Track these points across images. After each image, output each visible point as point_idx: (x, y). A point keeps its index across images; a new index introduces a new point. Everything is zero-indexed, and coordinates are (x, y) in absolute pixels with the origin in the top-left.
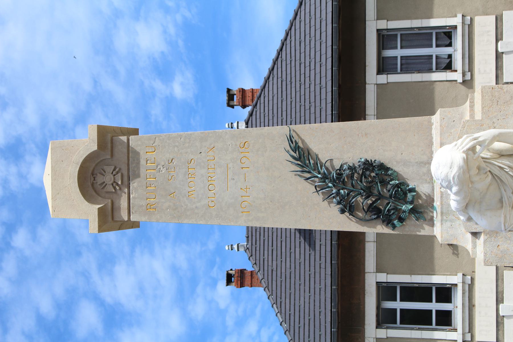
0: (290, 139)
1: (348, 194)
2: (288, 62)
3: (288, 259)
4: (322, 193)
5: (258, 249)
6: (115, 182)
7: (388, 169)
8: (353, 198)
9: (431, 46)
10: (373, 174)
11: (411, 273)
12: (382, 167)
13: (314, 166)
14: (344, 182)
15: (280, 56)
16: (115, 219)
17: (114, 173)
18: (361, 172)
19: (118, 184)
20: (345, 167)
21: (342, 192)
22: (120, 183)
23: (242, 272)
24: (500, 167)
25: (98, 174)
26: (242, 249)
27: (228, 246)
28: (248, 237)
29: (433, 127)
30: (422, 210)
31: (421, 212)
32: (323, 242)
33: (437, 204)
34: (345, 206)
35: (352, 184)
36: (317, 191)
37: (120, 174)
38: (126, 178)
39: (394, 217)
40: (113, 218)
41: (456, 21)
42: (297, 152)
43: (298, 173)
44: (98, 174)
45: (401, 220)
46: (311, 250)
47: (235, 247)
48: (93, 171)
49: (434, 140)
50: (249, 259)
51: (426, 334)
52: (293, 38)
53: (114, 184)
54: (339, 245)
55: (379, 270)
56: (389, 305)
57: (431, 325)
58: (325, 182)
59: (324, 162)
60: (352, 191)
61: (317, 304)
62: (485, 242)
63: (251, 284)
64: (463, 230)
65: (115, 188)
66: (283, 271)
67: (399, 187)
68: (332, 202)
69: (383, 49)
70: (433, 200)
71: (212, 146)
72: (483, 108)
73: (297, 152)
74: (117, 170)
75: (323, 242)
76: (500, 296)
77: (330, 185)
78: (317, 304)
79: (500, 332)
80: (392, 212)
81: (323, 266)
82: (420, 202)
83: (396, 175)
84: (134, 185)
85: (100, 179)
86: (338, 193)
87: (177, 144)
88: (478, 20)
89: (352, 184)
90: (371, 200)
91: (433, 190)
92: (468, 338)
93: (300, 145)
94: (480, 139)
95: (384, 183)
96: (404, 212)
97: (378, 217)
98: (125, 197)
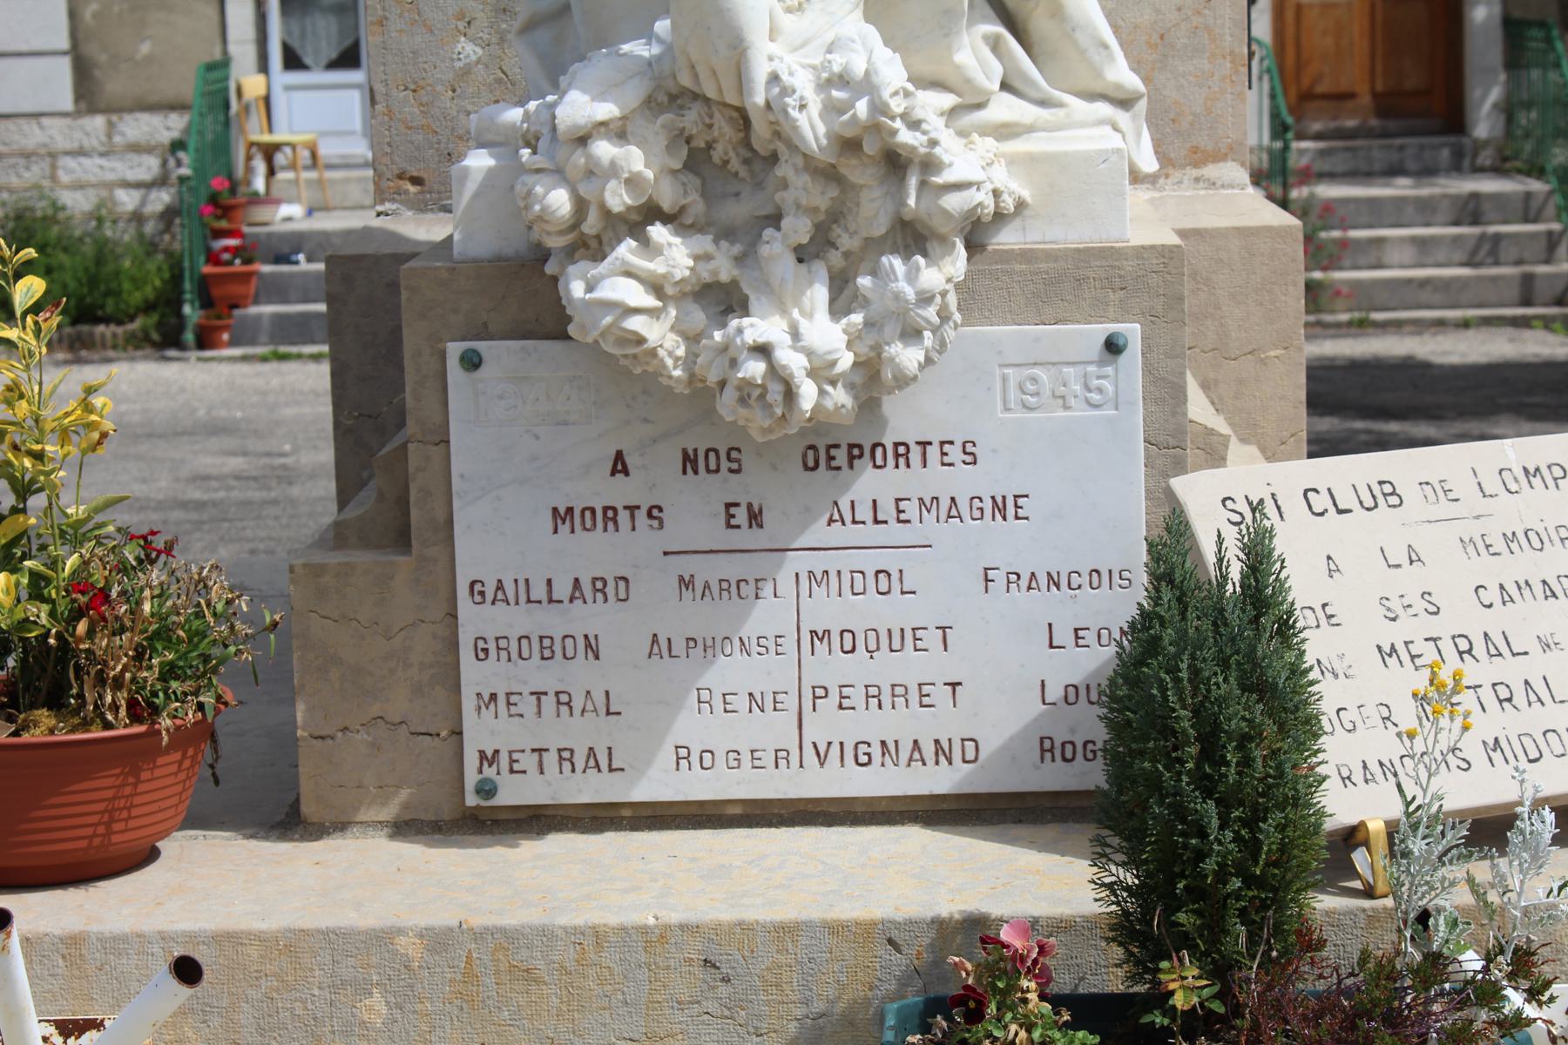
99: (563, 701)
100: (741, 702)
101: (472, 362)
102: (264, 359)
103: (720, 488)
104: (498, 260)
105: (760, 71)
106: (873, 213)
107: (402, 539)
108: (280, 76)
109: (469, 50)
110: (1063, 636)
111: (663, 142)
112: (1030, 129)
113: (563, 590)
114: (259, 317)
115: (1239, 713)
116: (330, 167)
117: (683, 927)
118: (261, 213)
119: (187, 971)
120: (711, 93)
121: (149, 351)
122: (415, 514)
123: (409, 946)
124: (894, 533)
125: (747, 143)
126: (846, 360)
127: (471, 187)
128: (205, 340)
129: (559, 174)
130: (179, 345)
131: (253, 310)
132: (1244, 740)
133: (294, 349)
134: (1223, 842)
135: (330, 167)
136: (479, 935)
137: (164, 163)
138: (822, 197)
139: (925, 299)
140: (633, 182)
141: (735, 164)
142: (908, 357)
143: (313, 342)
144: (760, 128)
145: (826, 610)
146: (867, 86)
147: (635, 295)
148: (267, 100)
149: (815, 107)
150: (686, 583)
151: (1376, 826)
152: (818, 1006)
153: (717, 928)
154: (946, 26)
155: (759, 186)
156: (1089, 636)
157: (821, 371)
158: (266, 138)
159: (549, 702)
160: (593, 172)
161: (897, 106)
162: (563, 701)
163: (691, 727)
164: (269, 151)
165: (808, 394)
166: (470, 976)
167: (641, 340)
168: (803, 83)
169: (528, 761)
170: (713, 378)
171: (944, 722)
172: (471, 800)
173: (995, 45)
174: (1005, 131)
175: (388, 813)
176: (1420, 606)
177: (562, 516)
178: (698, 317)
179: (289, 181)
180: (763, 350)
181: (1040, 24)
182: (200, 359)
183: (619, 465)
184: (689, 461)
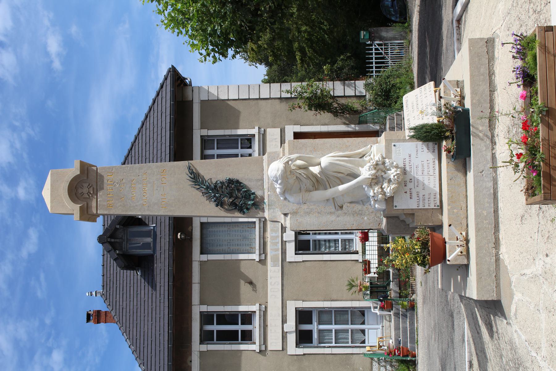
0: (189, 168)
1: (220, 196)
2: (137, 157)
3: (135, 299)
4: (206, 196)
5: (111, 294)
6: (89, 192)
7: (241, 183)
8: (223, 198)
9: (238, 148)
10: (233, 186)
11: (224, 304)
12: (238, 181)
13: (202, 182)
14: (218, 190)
15: (130, 154)
16: (89, 213)
17: (89, 187)
18: (226, 185)
19: (90, 193)
20: (218, 182)
21: (217, 195)
22: (92, 193)
23: (98, 313)
24: (299, 173)
25: (79, 188)
26: (99, 295)
27: (89, 293)
28: (103, 286)
29: (264, 161)
30: (259, 204)
31: (258, 205)
32: (162, 284)
33: (266, 201)
34: (218, 203)
35: (222, 191)
36: (203, 195)
37: (92, 188)
38: (95, 190)
39: (244, 207)
40: (87, 213)
41: (255, 131)
42: (193, 175)
43: (193, 186)
44: (79, 188)
45: (248, 209)
46: (153, 291)
47: (94, 293)
48: (76, 186)
49: (264, 168)
50: (104, 302)
51: (234, 347)
52: (140, 141)
53: (89, 193)
54: (174, 286)
55: (202, 303)
56: (209, 328)
57: (238, 340)
58: (207, 190)
59: (207, 180)
60: (222, 195)
61: (158, 328)
62: (290, 218)
63: (105, 321)
64: (280, 213)
65: (89, 195)
66: (131, 308)
67: (246, 192)
68: (211, 201)
69: (205, 149)
70: (264, 199)
71: (145, 172)
72: (289, 151)
73: (193, 175)
74: (90, 185)
75: (162, 284)
76: (284, 318)
77: (210, 191)
78: (158, 328)
79: (285, 343)
80: (243, 205)
81: (162, 301)
82: (257, 200)
83: (244, 186)
84: (100, 194)
85: (80, 191)
86: (215, 196)
87: (125, 171)
88: (268, 130)
89: (222, 191)
90: (232, 199)
91: (264, 193)
92: (263, 348)
93: (194, 171)
94: (291, 158)
95: (239, 190)
96: (249, 205)
97: (236, 208)
98: (95, 200)
99: (429, 198)
100: (429, 181)
101: (396, 206)
102: (418, 344)
103: (408, 184)
104: (386, 204)
105: (368, 177)
106: (381, 167)
107: (413, 214)
108: (366, 344)
109: (366, 218)
110: (422, 150)
111: (375, 186)
112: (374, 154)
113: (418, 198)
114: (410, 346)
115: (424, 130)
116: (383, 336)
117: (447, 182)
118: (391, 347)
119: (450, 225)
120: (370, 182)
121: (416, 368)
122: (411, 213)
123: (449, 207)
124: (412, 166)
125: (375, 179)
126: (395, 169)
127: (379, 206)
128: (414, 356)
129: (378, 196)
130: (415, 361)
131: (409, 347)
132: (427, 129)
133: (416, 339)
134: (436, 131)
135: (383, 336)
136: (448, 201)
137: (382, 366)
138: (380, 171)
139: (389, 162)
140: (378, 189)
141: (377, 180)
142: (395, 163)
143: (415, 336)
144: (373, 177)
145: (420, 173)
146: (370, 166)
147: (389, 188)
148: (370, 346)
149: (372, 171)
150: (417, 186)
151: (437, 119)
152: (455, 169)
153: (447, 179)
154: (364, 161)
155: (379, 178)
156: (422, 148)
157: (396, 171)
158: (377, 347)
159: (429, 200)
160: (378, 193)
161: (372, 164)
162: (429, 198)
163: (432, 186)
164: (380, 347)
165: (398, 172)
166: (452, 202)
167: (393, 188)
168: (369, 173)
169: (435, 202)
170: (397, 182)
171: (431, 162)
172: (439, 208)
173: (366, 157)
174: (374, 156)
175: (440, 216)
176: (418, 116)
177: (411, 198)
178: (391, 183)
179: (385, 343)
180: (394, 176)
181: (364, 153)
182: (418, 357)
183: (406, 192)
184: (405, 186)
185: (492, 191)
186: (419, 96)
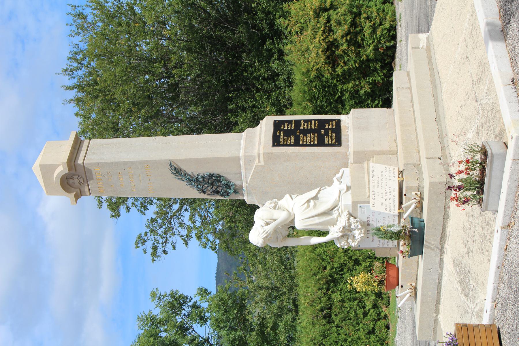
29: (241, 160)
33: (245, 188)
38: (85, 180)
70: (243, 187)
91: (242, 183)
93: (176, 167)
95: (219, 181)
123: (403, 269)
174: (342, 211)
185: (437, 281)
186: (384, 174)
